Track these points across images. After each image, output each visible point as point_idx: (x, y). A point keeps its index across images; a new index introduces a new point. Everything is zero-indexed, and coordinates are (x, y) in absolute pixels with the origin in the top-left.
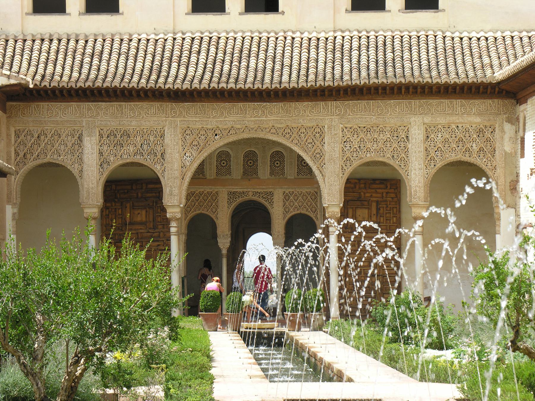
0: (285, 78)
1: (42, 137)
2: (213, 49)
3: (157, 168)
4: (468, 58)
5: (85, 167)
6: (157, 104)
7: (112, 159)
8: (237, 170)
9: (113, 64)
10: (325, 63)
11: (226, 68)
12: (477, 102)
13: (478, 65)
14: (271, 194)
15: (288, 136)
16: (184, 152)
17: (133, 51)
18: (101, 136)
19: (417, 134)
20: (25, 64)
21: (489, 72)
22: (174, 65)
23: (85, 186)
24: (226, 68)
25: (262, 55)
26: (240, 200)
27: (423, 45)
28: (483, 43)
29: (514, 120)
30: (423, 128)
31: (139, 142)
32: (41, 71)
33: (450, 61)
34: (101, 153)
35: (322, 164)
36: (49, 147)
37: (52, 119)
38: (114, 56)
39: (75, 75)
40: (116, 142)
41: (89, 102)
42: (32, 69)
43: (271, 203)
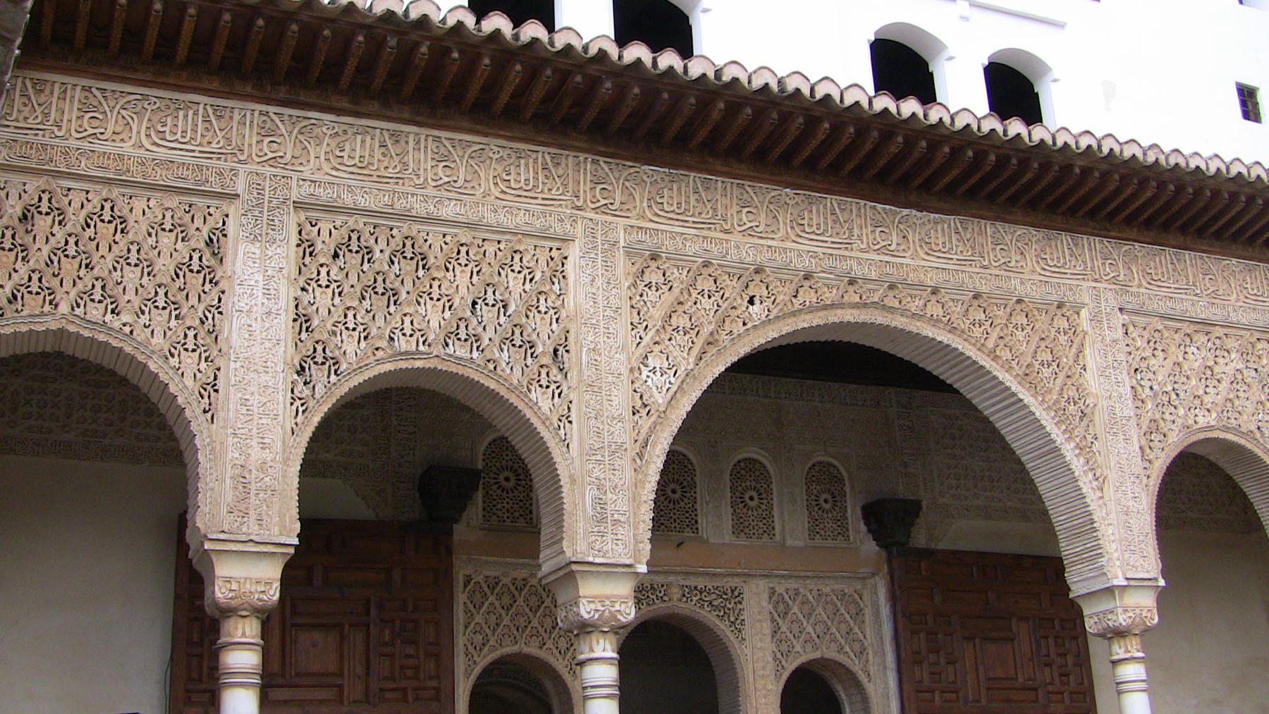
1: (42, 223)
3: (540, 406)
5: (232, 372)
6: (544, 154)
7: (350, 347)
14: (736, 595)
15: (977, 332)
16: (641, 350)
18: (307, 248)
23: (232, 454)
31: (463, 290)
34: (303, 321)
35: (1089, 438)
36: (69, 267)
37: (101, 149)
40: (368, 279)
41: (268, 102)
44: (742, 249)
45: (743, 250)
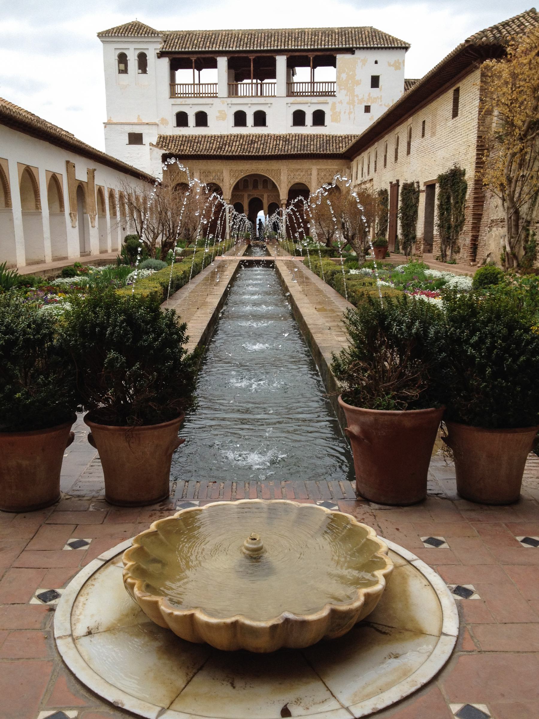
0: (267, 151)
2: (241, 140)
3: (221, 185)
4: (334, 144)
6: (220, 161)
8: (251, 188)
9: (205, 146)
10: (282, 145)
11: (246, 147)
12: (336, 161)
13: (338, 146)
14: (263, 195)
17: (212, 141)
19: (314, 173)
20: (173, 145)
21: (341, 149)
22: (227, 146)
24: (246, 147)
25: (259, 143)
26: (251, 197)
27: (318, 139)
28: (340, 139)
29: (350, 168)
30: (316, 170)
32: (179, 148)
33: (328, 145)
38: (206, 143)
39: (191, 149)
42: (176, 147)
43: (263, 199)
44: (241, 168)
45: (241, 168)
